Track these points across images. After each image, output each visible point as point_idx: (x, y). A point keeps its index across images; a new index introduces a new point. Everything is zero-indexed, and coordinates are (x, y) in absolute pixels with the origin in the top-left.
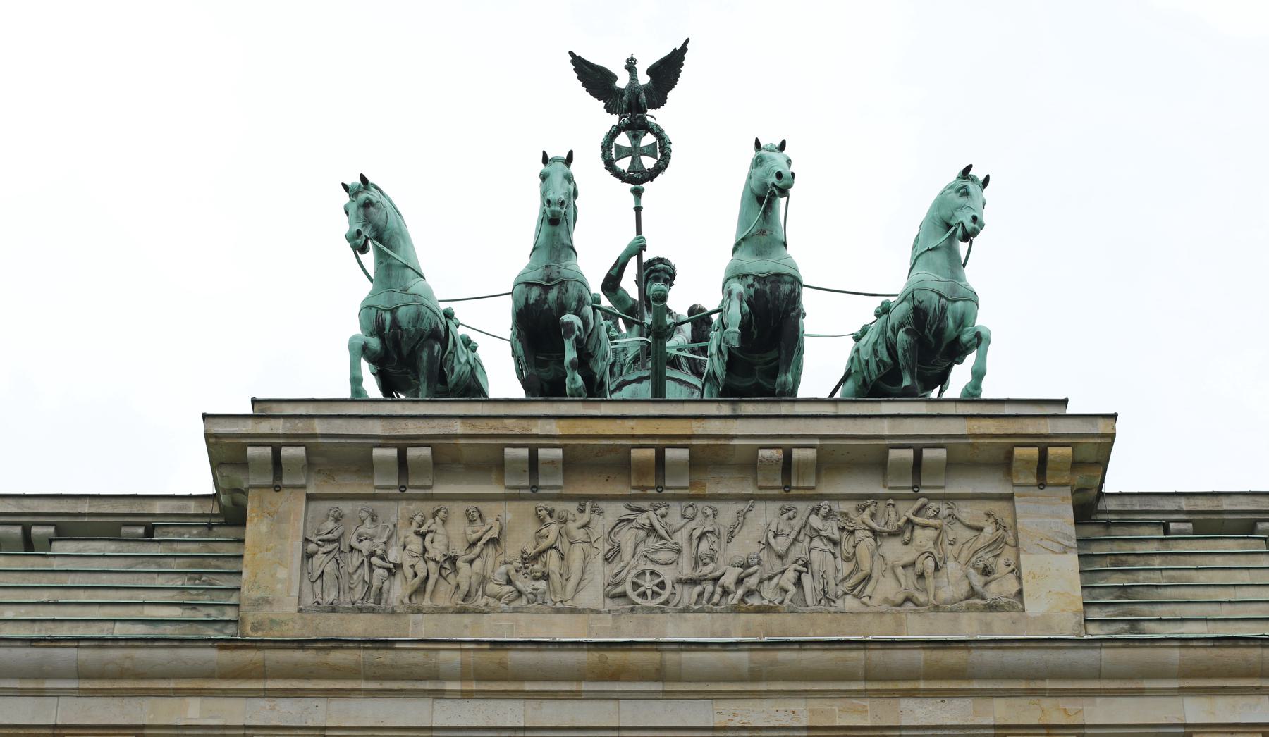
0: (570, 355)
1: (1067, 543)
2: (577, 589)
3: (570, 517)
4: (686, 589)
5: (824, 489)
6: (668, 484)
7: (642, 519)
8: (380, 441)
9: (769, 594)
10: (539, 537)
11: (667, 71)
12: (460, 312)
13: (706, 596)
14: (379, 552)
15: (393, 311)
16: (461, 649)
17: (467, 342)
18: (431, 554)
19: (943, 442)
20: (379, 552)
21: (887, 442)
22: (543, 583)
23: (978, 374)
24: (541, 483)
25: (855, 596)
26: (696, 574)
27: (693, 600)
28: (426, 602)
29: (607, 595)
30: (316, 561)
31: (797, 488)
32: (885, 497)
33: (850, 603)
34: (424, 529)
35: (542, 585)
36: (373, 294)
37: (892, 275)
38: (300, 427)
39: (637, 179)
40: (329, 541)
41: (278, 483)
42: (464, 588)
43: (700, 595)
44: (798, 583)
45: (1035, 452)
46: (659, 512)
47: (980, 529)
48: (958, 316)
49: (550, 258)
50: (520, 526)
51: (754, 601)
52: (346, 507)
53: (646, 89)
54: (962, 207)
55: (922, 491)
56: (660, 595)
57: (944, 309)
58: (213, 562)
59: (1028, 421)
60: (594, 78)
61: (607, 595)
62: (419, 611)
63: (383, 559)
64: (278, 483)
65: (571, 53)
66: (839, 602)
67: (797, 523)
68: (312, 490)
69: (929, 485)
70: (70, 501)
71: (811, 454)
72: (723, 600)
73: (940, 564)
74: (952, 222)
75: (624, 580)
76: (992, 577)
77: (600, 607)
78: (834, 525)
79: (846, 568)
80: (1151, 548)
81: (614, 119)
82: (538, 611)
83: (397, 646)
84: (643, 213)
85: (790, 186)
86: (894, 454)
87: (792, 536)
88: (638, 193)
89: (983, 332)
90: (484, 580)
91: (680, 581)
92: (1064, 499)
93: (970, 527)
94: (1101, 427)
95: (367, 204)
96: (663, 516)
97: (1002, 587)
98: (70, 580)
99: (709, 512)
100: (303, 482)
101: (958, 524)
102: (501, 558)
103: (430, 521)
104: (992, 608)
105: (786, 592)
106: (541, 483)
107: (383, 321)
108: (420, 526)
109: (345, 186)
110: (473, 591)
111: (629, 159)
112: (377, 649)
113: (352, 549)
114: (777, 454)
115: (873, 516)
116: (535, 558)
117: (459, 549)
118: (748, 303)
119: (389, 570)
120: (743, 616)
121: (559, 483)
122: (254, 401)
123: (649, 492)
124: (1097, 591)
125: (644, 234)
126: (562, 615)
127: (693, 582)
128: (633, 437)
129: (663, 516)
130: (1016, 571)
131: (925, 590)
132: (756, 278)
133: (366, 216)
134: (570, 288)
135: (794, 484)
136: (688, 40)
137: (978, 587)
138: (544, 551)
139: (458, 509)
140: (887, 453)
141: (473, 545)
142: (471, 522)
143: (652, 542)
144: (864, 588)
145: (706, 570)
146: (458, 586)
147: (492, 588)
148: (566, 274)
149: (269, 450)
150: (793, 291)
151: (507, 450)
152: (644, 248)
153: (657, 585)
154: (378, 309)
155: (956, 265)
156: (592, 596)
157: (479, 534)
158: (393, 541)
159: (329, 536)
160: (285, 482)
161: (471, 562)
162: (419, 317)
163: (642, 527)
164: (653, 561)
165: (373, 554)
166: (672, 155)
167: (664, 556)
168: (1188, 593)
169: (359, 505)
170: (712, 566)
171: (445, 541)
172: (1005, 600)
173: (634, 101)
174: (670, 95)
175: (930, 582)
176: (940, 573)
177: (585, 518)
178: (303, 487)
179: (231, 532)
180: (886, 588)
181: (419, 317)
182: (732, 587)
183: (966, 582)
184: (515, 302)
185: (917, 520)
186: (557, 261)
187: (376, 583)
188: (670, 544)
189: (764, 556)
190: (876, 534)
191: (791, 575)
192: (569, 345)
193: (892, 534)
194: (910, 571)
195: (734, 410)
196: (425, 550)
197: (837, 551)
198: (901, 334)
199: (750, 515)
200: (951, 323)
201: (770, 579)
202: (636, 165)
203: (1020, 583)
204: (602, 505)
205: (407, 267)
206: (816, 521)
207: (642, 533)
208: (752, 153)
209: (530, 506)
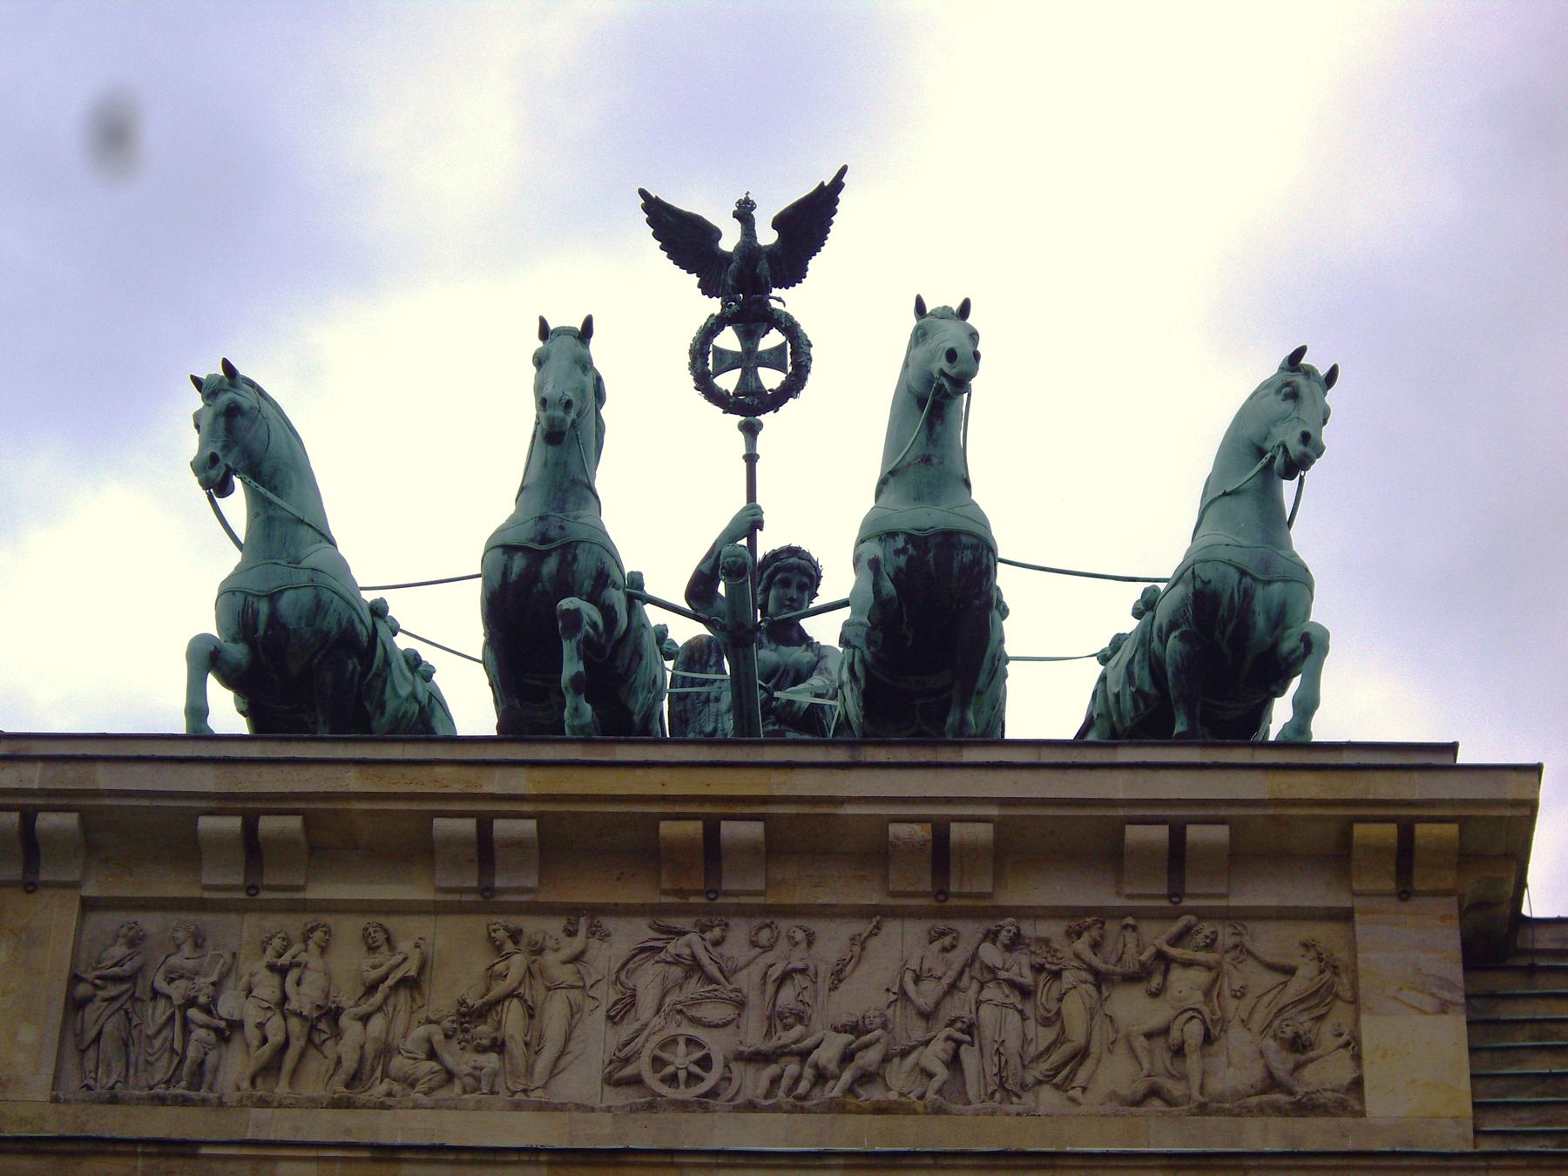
0: (571, 666)
1: (1447, 996)
2: (554, 1071)
3: (550, 943)
5: (1007, 899)
6: (726, 886)
7: (676, 947)
8: (213, 804)
9: (899, 1079)
10: (492, 976)
11: (809, 222)
12: (400, 607)
13: (785, 1082)
14: (202, 999)
15: (273, 597)
16: (318, 1159)
17: (413, 661)
19: (1223, 812)
20: (202, 999)
21: (1121, 812)
22: (493, 1057)
23: (1306, 706)
24: (499, 882)
27: (761, 1091)
28: (282, 1089)
29: (609, 1081)
30: (91, 1012)
31: (960, 895)
32: (1119, 914)
33: (1048, 1096)
34: (286, 959)
35: (491, 1061)
36: (239, 571)
37: (1162, 538)
38: (70, 778)
39: (750, 406)
42: (350, 1063)
43: (775, 1081)
44: (954, 1062)
45: (1390, 830)
46: (708, 935)
47: (1290, 971)
50: (459, 958)
51: (875, 1094)
52: (151, 923)
53: (770, 252)
54: (1284, 418)
55: (1187, 903)
56: (700, 1079)
57: (1248, 596)
59: (1378, 777)
60: (681, 236)
61: (609, 1081)
63: (208, 1010)
65: (643, 193)
66: (1028, 1098)
67: (958, 957)
68: (90, 890)
69: (1200, 893)
71: (984, 832)
72: (816, 1091)
73: (1215, 1032)
74: (1268, 446)
75: (638, 1053)
76: (1312, 1054)
77: (596, 1102)
79: (1046, 1036)
81: (714, 306)
82: (478, 1107)
83: (204, 1150)
84: (759, 465)
85: (972, 374)
86: (1133, 833)
87: (946, 981)
88: (751, 431)
89: (1314, 633)
90: (386, 1051)
92: (1443, 918)
93: (1272, 967)
94: (1512, 789)
95: (232, 412)
96: (717, 943)
99: (800, 936)
100: (75, 875)
101: (1251, 962)
102: (421, 1015)
104: (1306, 1107)
105: (931, 1076)
106: (499, 882)
107: (256, 614)
108: (280, 956)
109: (197, 382)
110: (368, 1067)
111: (739, 371)
112: (168, 1156)
113: (156, 994)
114: (921, 832)
115: (1096, 946)
116: (481, 1014)
117: (346, 997)
119: (218, 1031)
120: (851, 1121)
121: (532, 881)
123: (692, 900)
124: (1502, 1083)
125: (758, 502)
126: (523, 1115)
127: (759, 1058)
128: (664, 799)
129: (717, 943)
130: (1353, 1046)
131: (1184, 1077)
132: (910, 538)
133: (229, 429)
134: (581, 556)
135: (954, 888)
136: (844, 170)
137: (1281, 1073)
138: (499, 1001)
139: (348, 928)
140: (1122, 832)
141: (371, 989)
142: (373, 949)
143: (694, 987)
144: (1074, 1072)
145: (788, 1037)
146: (339, 1061)
147: (398, 1064)
148: (576, 531)
151: (438, 823)
152: (758, 524)
154: (247, 594)
155: (1275, 522)
156: (582, 1080)
157: (383, 969)
158: (230, 982)
160: (44, 876)
161: (365, 1019)
162: (319, 607)
163: (677, 960)
165: (191, 1002)
166: (814, 366)
167: (712, 1012)
169: (173, 918)
170: (798, 1030)
172: (1329, 1095)
173: (749, 276)
174: (814, 264)
175: (1193, 1063)
176: (1215, 1047)
177: (577, 944)
178: (75, 885)
180: (1115, 1073)
181: (319, 607)
182: (833, 1067)
183: (1261, 1063)
184: (485, 585)
185: (1174, 952)
187: (192, 1053)
188: (726, 990)
189: (896, 1015)
192: (569, 648)
194: (1159, 1043)
196: (285, 998)
197: (1028, 1008)
198: (1173, 640)
199: (874, 943)
200: (1261, 621)
201: (904, 1054)
202: (749, 387)
204: (609, 923)
205: (302, 522)
206: (991, 954)
207: (677, 972)
208: (911, 322)
209: (477, 924)
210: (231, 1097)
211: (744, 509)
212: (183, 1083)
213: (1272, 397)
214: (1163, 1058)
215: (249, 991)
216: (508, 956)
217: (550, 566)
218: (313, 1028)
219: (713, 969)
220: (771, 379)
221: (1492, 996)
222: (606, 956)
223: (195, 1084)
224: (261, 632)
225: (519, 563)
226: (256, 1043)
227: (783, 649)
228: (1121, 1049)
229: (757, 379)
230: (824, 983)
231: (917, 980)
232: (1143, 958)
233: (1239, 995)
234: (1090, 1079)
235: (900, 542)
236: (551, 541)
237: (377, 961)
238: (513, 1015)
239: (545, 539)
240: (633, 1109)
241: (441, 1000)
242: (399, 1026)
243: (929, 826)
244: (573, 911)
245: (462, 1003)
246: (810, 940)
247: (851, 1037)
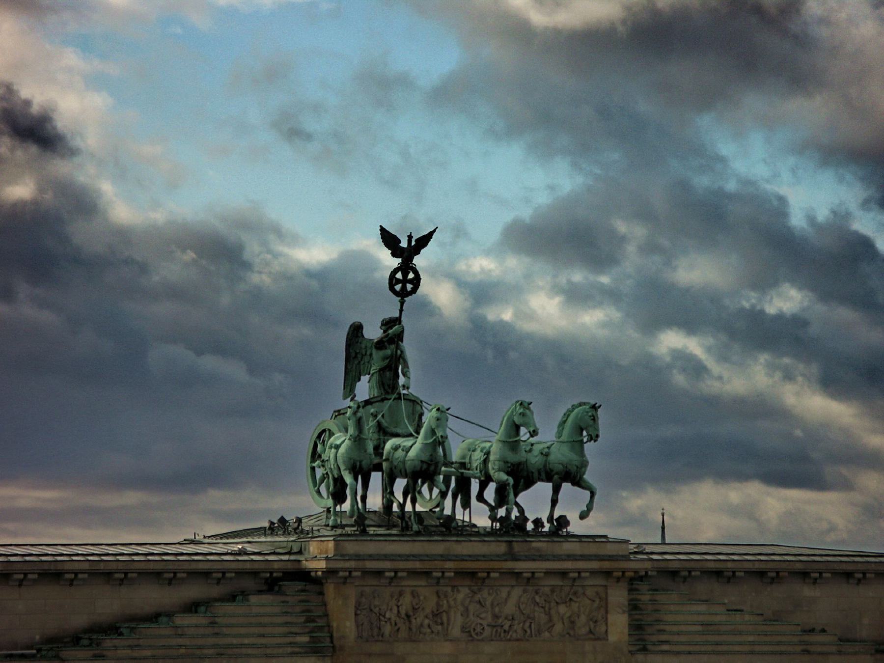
7: (478, 597)
10: (438, 604)
11: (424, 241)
25: (550, 632)
26: (493, 624)
33: (547, 634)
35: (440, 627)
38: (360, 564)
44: (530, 626)
60: (389, 239)
81: (396, 262)
88: (402, 303)
90: (422, 625)
104: (596, 639)
111: (400, 285)
126: (447, 643)
131: (573, 629)
139: (408, 590)
142: (414, 597)
156: (456, 632)
164: (481, 618)
167: (483, 616)
174: (422, 251)
185: (575, 599)
190: (557, 603)
191: (527, 624)
204: (460, 588)
206: (537, 599)
213: (587, 418)
215: (391, 609)
217: (432, 468)
220: (409, 287)
222: (460, 596)
225: (425, 466)
238: (445, 619)
239: (432, 461)
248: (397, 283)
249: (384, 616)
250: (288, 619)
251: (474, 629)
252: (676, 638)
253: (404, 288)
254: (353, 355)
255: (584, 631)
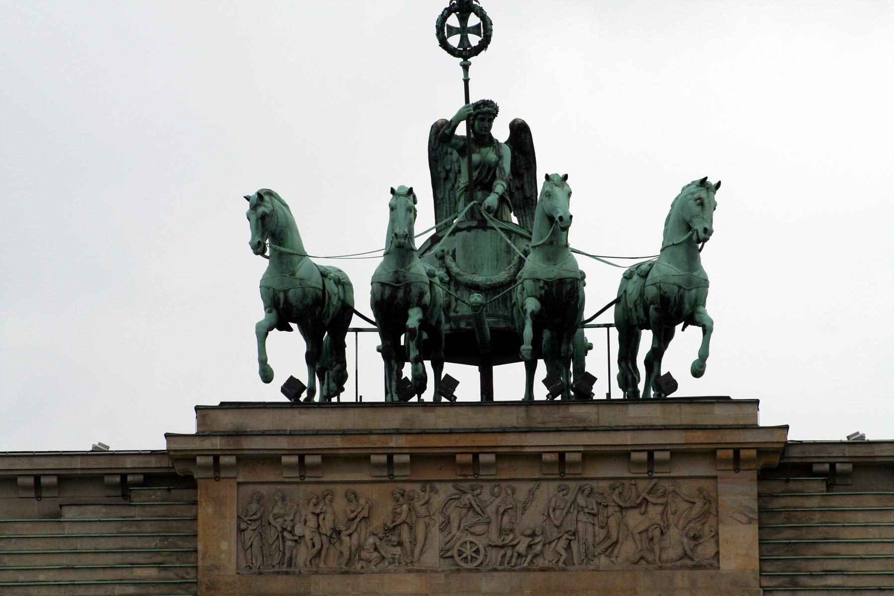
1: (751, 516)
2: (422, 552)
3: (416, 496)
4: (495, 549)
10: (395, 514)
13: (507, 558)
14: (289, 529)
15: (286, 292)
18: (324, 531)
20: (289, 529)
24: (396, 473)
25: (609, 556)
26: (500, 543)
30: (248, 534)
33: (604, 560)
34: (318, 511)
35: (398, 550)
39: (465, 53)
40: (255, 520)
41: (217, 474)
42: (346, 554)
43: (504, 556)
44: (568, 548)
46: (476, 492)
47: (694, 503)
48: (692, 301)
49: (398, 264)
51: (540, 562)
52: (264, 490)
54: (697, 216)
55: (655, 475)
57: (682, 297)
58: (175, 524)
59: (726, 432)
62: (316, 573)
63: (291, 532)
64: (217, 474)
66: (596, 560)
67: (569, 498)
68: (240, 480)
69: (658, 472)
70: (66, 458)
72: (519, 560)
75: (452, 548)
78: (594, 503)
79: (602, 534)
80: (814, 503)
82: (395, 572)
87: (565, 511)
88: (466, 67)
89: (708, 324)
90: (360, 547)
91: (490, 545)
92: (751, 480)
94: (777, 437)
95: (263, 217)
97: (706, 550)
98: (80, 545)
99: (509, 492)
102: (371, 529)
103: (321, 505)
104: (698, 567)
105: (561, 555)
107: (279, 299)
108: (315, 505)
109: (247, 198)
111: (459, 36)
113: (270, 524)
115: (620, 494)
118: (540, 299)
119: (296, 541)
120: (532, 575)
122: (197, 408)
123: (469, 478)
126: (412, 575)
131: (652, 551)
132: (545, 282)
133: (263, 225)
135: (567, 472)
137: (689, 552)
139: (340, 490)
142: (349, 501)
143: (471, 518)
144: (612, 552)
146: (341, 553)
147: (364, 554)
148: (410, 277)
149: (211, 459)
150: (573, 288)
153: (475, 552)
156: (431, 558)
157: (355, 513)
158: (297, 517)
159: (255, 517)
161: (350, 535)
162: (305, 295)
163: (464, 506)
164: (473, 534)
165: (284, 529)
167: (478, 529)
168: (834, 549)
170: (511, 536)
171: (332, 518)
175: (657, 549)
179: (186, 494)
180: (628, 549)
182: (524, 553)
184: (373, 293)
186: (403, 266)
187: (288, 555)
191: (563, 543)
193: (632, 507)
195: (527, 411)
196: (319, 525)
197: (596, 519)
199: (538, 492)
200: (687, 306)
201: (550, 543)
203: (718, 546)
204: (438, 486)
206: (581, 501)
207: (464, 511)
209: (390, 487)
210: (304, 571)
211: (464, 108)
212: (285, 565)
213: (692, 203)
214: (645, 544)
215: (305, 522)
216: (401, 505)
217: (401, 294)
218: (330, 537)
219: (478, 510)
220: (474, 40)
221: (772, 496)
222: (438, 500)
223: (290, 565)
224: (282, 305)
225: (388, 292)
226: (310, 546)
227: (484, 150)
228: (630, 538)
229: (468, 41)
230: (519, 512)
231: (554, 510)
232: (638, 502)
233: (674, 513)
234: (619, 552)
235: (542, 284)
236: (400, 282)
237: (353, 508)
238: (405, 535)
240: (452, 572)
241: (377, 523)
242: (363, 537)
243: (557, 455)
244: (424, 482)
245: (385, 525)
246: (514, 491)
247: (530, 539)
248: (450, 35)
249: (291, 532)
250: (128, 543)
251: (460, 553)
252: (858, 566)
253: (464, 41)
254: (443, 175)
255: (672, 553)
